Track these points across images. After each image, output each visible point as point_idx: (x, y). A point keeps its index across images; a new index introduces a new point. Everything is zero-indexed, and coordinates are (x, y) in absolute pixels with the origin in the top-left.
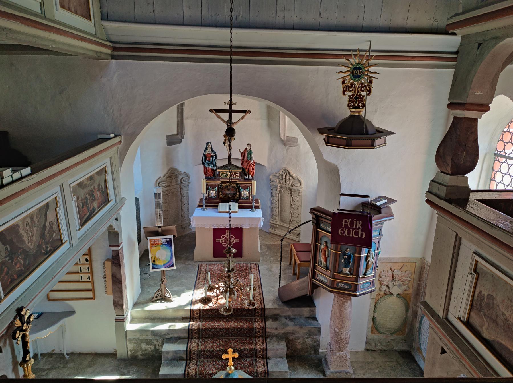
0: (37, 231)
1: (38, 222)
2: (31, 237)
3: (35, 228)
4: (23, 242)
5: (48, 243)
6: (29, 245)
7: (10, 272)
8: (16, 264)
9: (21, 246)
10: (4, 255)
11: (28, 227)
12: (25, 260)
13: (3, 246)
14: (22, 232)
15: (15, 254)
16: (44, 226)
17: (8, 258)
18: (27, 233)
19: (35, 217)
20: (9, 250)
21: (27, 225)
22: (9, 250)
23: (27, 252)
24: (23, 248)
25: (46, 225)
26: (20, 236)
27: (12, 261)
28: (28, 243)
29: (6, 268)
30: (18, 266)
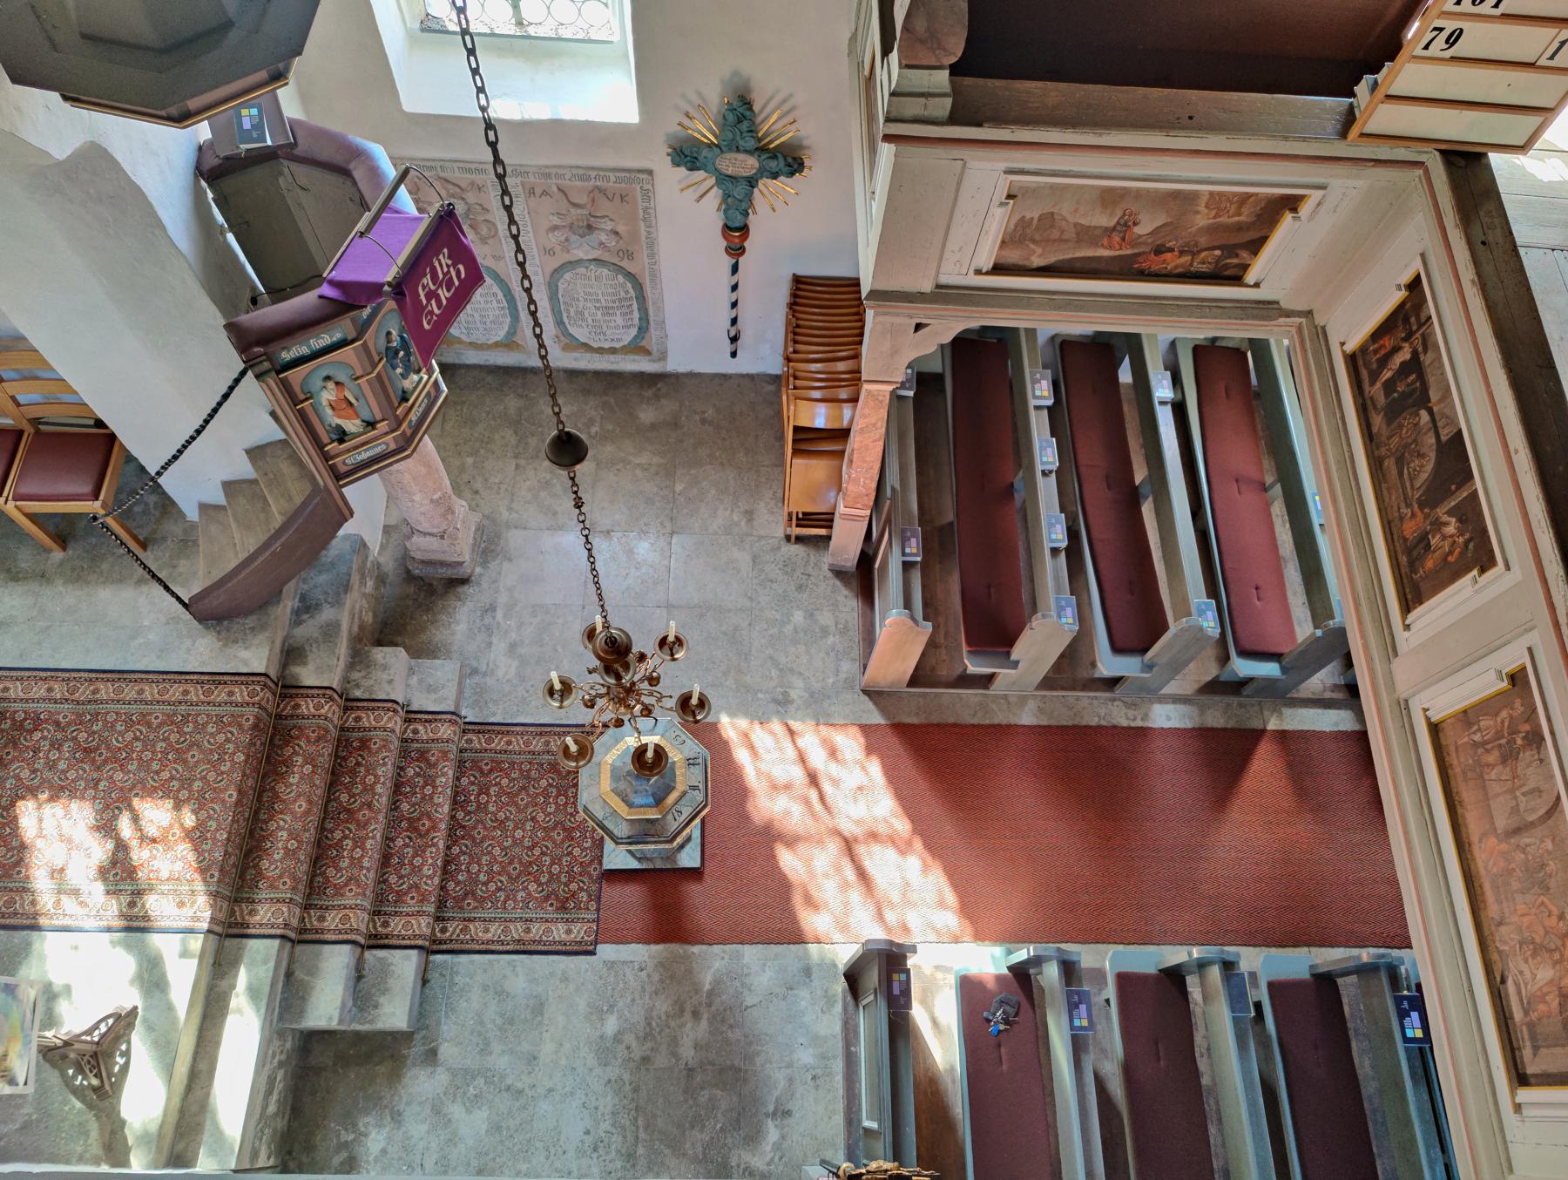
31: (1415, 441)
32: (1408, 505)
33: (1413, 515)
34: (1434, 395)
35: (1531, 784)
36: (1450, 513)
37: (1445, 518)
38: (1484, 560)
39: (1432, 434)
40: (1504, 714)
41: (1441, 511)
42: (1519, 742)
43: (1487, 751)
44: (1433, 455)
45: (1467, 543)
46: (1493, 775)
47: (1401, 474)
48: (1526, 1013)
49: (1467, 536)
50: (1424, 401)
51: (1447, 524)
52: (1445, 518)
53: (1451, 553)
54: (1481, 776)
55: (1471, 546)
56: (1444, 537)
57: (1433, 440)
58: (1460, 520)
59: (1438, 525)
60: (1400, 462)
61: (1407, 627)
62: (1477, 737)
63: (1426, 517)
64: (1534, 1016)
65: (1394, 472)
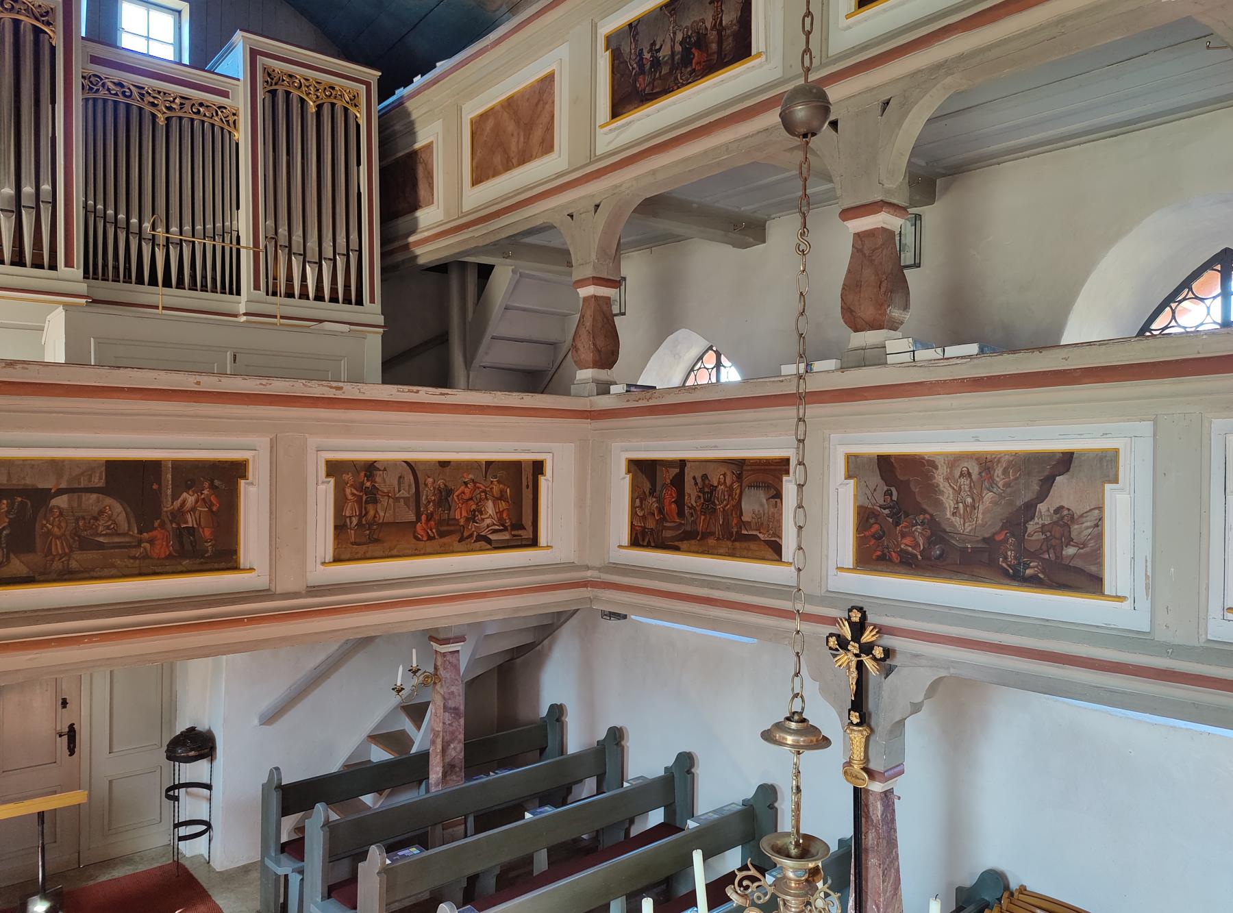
0: (995, 503)
1: (1007, 485)
2: (966, 506)
3: (988, 496)
4: (939, 504)
5: (1034, 555)
6: (957, 521)
7: (885, 541)
8: (903, 536)
9: (930, 510)
10: (882, 502)
11: (964, 482)
12: (930, 542)
13: (881, 482)
14: (939, 478)
15: (907, 515)
16: (1029, 509)
17: (887, 511)
18: (958, 492)
19: (999, 471)
20: (895, 498)
21: (962, 475)
22: (895, 498)
23: (945, 531)
24: (931, 515)
25: (1042, 507)
26: (931, 489)
27: (897, 524)
28: (954, 514)
29: (876, 526)
30: (907, 540)
31: (77, 520)
32: (139, 546)
33: (151, 541)
34: (48, 483)
35: (396, 483)
36: (175, 497)
37: (178, 503)
38: (234, 471)
39: (85, 496)
40: (348, 491)
41: (169, 506)
42: (368, 484)
43: (367, 513)
44: (109, 501)
45: (213, 487)
46: (382, 514)
47: (101, 546)
48: (505, 529)
49: (206, 484)
50: (41, 497)
51: (184, 502)
52: (178, 503)
53: (212, 504)
54: (378, 524)
55: (217, 483)
56: (193, 509)
57: (94, 496)
58: (187, 488)
59: (179, 514)
60: (86, 544)
61: (252, 569)
62: (355, 521)
63: (162, 525)
64: (508, 523)
65: (93, 555)
